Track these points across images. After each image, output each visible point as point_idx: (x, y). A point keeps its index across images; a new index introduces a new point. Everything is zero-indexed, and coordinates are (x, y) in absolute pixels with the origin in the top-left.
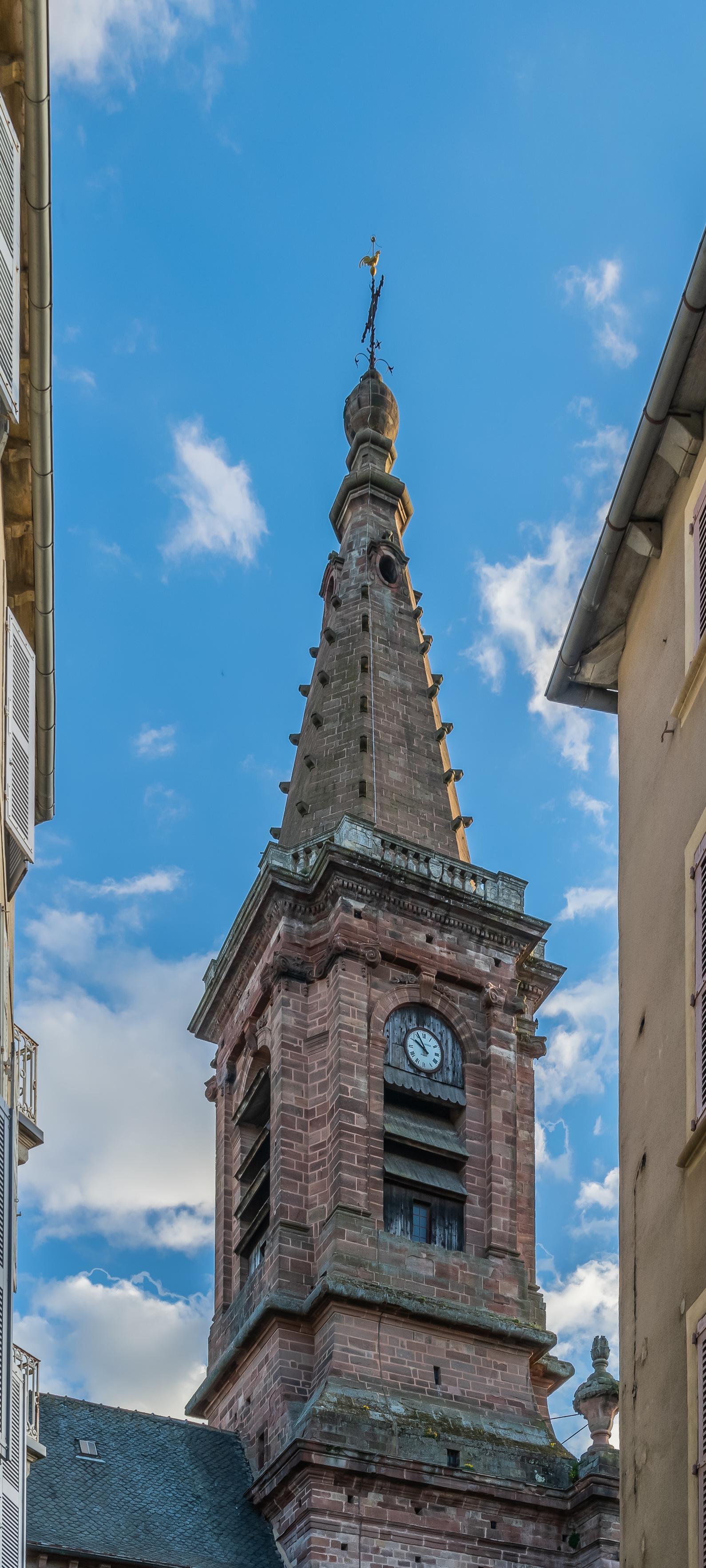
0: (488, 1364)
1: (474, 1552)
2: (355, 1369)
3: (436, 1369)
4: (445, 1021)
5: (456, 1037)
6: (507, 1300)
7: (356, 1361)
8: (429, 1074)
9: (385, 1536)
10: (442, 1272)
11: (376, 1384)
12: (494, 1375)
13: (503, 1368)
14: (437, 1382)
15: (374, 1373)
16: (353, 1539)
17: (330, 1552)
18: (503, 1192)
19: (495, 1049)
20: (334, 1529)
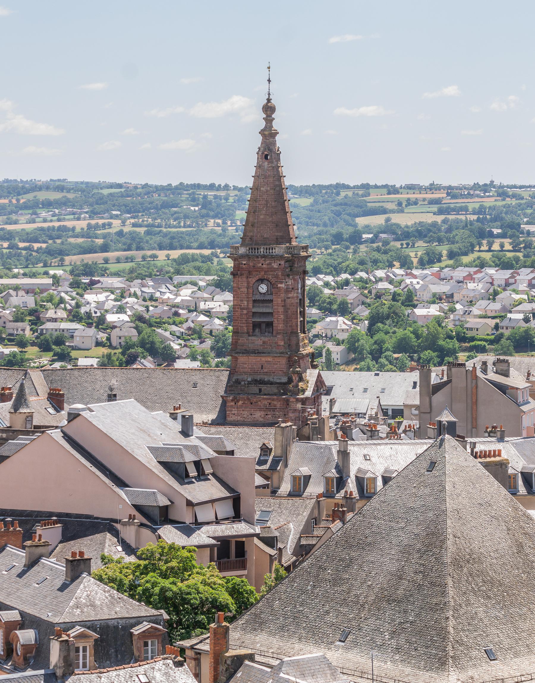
0: (275, 362)
1: (264, 411)
2: (242, 370)
3: (262, 366)
4: (268, 280)
5: (271, 283)
6: (280, 346)
7: (242, 368)
8: (264, 294)
9: (243, 410)
10: (264, 342)
11: (246, 373)
12: (277, 364)
13: (279, 362)
14: (262, 368)
15: (246, 370)
16: (236, 412)
17: (231, 415)
18: (281, 319)
19: (279, 285)
20: (232, 410)
